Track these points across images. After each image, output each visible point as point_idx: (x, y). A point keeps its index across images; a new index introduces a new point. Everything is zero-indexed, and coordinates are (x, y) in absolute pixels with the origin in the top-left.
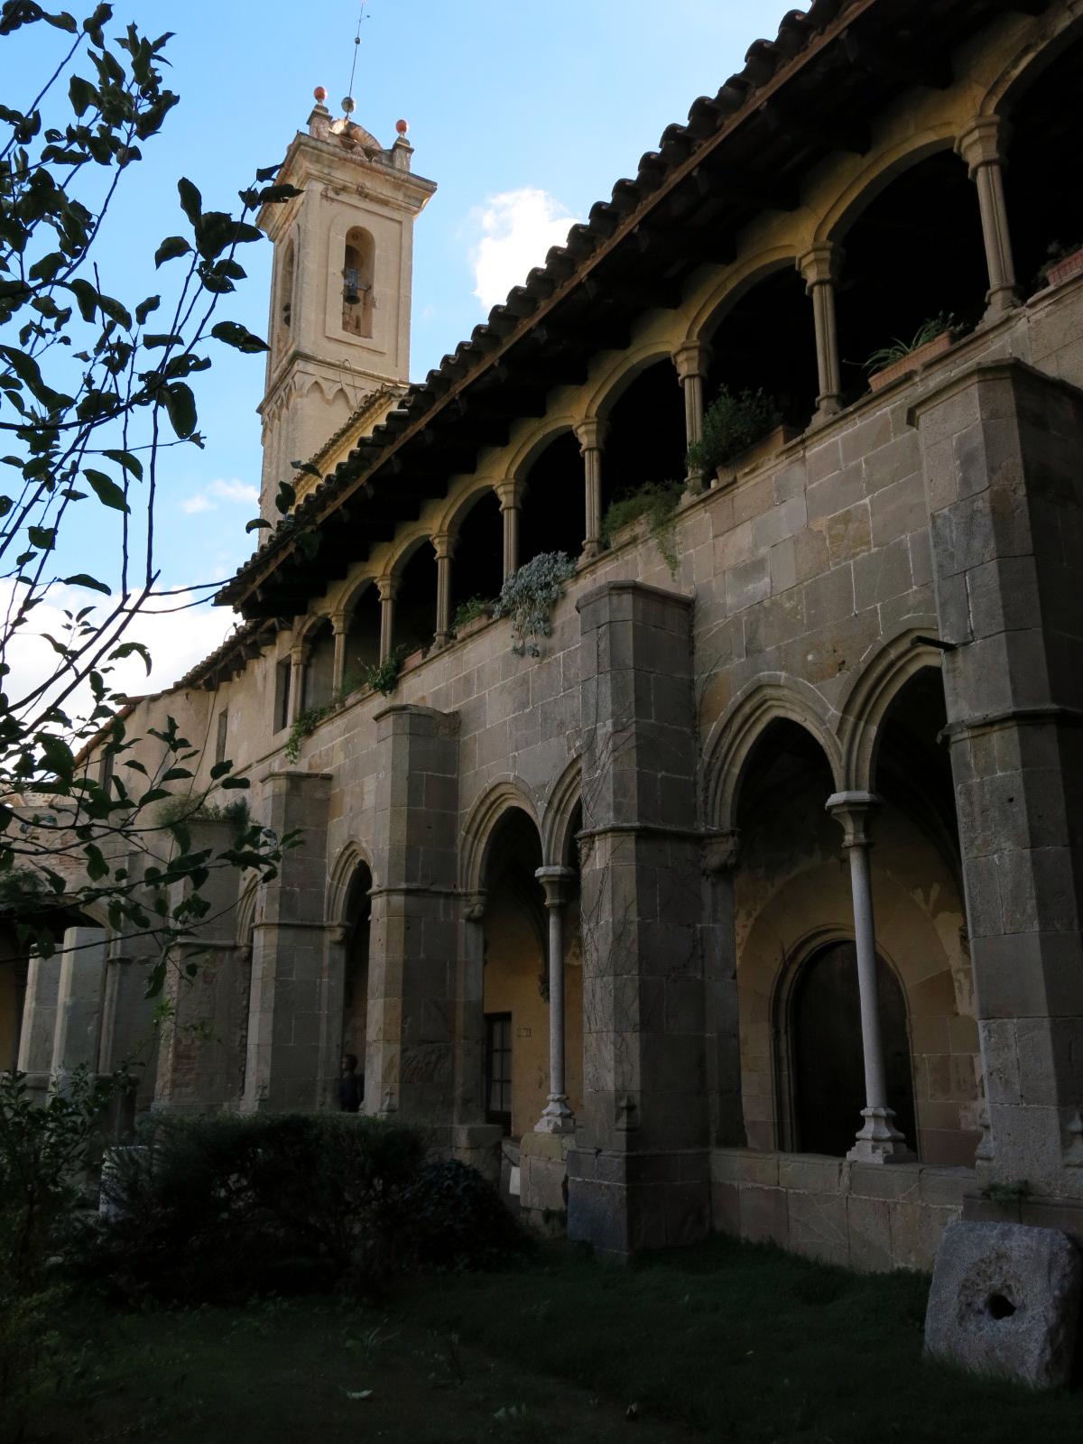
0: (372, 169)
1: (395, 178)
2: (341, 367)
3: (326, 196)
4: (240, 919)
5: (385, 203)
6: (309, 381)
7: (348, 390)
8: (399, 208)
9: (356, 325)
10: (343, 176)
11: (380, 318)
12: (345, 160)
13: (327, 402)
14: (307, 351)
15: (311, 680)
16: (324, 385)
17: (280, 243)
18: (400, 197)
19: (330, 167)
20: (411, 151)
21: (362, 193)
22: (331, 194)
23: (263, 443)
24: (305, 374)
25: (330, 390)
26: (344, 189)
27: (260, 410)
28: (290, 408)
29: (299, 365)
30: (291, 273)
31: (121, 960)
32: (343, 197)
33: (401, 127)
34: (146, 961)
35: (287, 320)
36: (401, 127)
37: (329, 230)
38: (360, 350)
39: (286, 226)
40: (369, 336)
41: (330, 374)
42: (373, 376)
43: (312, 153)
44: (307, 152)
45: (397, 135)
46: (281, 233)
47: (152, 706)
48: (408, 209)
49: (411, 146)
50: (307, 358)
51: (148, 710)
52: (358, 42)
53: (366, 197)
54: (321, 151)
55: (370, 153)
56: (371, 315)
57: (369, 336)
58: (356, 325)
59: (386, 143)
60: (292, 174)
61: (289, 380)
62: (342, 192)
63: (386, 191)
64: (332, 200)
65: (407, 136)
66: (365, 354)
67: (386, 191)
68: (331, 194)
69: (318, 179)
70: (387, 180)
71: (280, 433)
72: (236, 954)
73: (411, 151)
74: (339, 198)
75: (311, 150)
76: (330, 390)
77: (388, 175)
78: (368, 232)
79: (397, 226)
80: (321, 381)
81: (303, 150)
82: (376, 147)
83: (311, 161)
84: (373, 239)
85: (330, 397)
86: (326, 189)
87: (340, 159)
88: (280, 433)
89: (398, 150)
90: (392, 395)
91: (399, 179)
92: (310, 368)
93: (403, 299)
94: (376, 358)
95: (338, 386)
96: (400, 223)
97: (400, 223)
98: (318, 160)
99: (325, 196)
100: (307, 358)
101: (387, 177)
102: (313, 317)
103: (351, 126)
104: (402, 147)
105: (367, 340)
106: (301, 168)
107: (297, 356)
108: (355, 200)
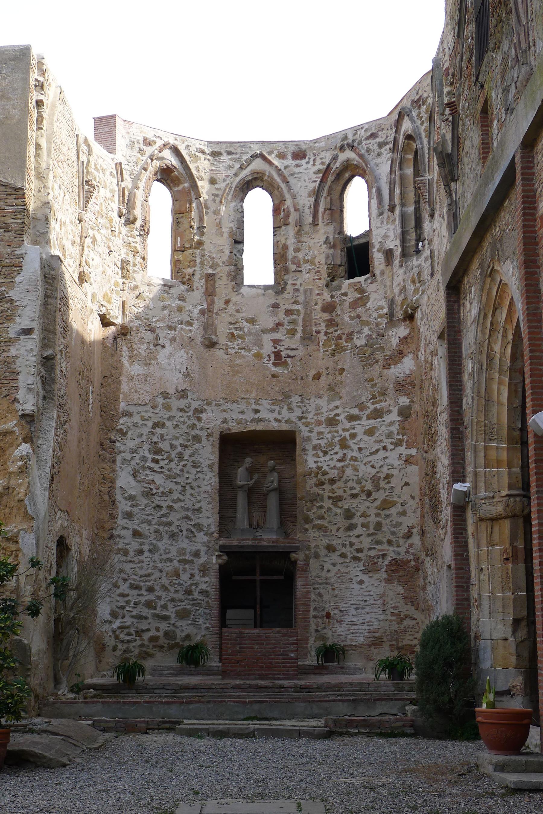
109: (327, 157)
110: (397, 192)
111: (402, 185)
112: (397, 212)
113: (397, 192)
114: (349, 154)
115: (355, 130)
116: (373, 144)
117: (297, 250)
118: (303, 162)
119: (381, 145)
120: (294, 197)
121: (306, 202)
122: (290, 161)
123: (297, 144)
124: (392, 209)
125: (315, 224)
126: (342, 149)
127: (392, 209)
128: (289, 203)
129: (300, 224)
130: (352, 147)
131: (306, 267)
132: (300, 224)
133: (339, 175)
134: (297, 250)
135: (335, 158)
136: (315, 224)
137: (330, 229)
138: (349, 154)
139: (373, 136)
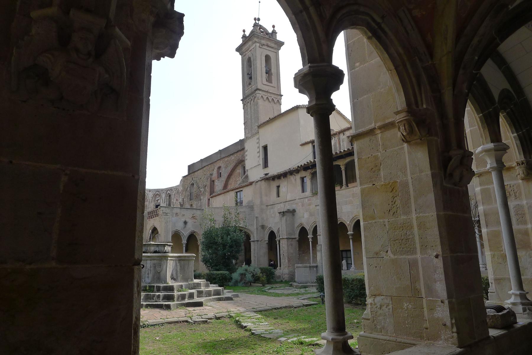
0: (270, 40)
1: (275, 41)
2: (267, 92)
3: (260, 47)
4: (296, 232)
5: (272, 48)
6: (261, 96)
7: (269, 97)
8: (275, 49)
9: (269, 80)
10: (263, 42)
11: (274, 78)
12: (264, 38)
13: (264, 101)
14: (259, 87)
15: (313, 183)
16: (264, 96)
17: (244, 56)
18: (276, 46)
19: (260, 39)
20: (277, 33)
21: (268, 46)
22: (261, 46)
23: (243, 109)
24: (259, 94)
25: (265, 98)
26: (264, 45)
27: (241, 100)
28: (255, 102)
29: (257, 92)
30: (251, 67)
31: (258, 241)
32: (264, 47)
33: (274, 27)
34: (261, 241)
35: (251, 78)
36: (274, 27)
37: (261, 56)
38: (270, 87)
39: (247, 52)
40: (272, 83)
41: (264, 93)
42: (274, 94)
43: (257, 36)
44: (256, 36)
45: (272, 29)
46: (244, 54)
47: (256, 183)
48: (278, 49)
49: (277, 32)
50: (259, 90)
51: (256, 184)
52: (260, 2)
53: (268, 46)
54: (259, 36)
55: (267, 33)
56: (272, 77)
57: (272, 83)
58: (269, 80)
59: (270, 30)
60: (250, 41)
61: (254, 94)
62: (263, 46)
63: (273, 45)
64: (261, 48)
65: (275, 29)
66: (271, 88)
67: (273, 45)
68: (261, 46)
69: (258, 42)
70: (273, 42)
71: (251, 108)
72: (296, 239)
73: (277, 33)
74: (262, 47)
75: (256, 36)
76: (265, 98)
77: (273, 41)
78: (269, 55)
79: (275, 53)
80: (263, 95)
81: (255, 36)
82: (267, 32)
83: (256, 39)
84: (271, 58)
85: (265, 100)
86: (260, 45)
87: (263, 37)
88: (251, 108)
89: (274, 33)
90: (299, 107)
91: (276, 42)
92: (260, 92)
93: (278, 73)
94: (274, 89)
95: (267, 96)
96: (276, 53)
97: (276, 53)
98: (258, 38)
99: (259, 47)
100: (259, 90)
101: (274, 41)
102: (260, 79)
103: (260, 26)
104: (274, 32)
105: (271, 84)
106: (253, 40)
107: (257, 89)
108: (266, 47)
109: (154, 192)
110: (166, 200)
111: (167, 200)
112: (166, 203)
113: (166, 200)
114: (158, 193)
115: (159, 189)
116: (162, 192)
117: (149, 205)
118: (150, 192)
119: (163, 192)
120: (149, 197)
121: (151, 199)
122: (148, 192)
123: (149, 189)
124: (165, 202)
125: (152, 202)
126: (157, 192)
127: (165, 202)
128: (148, 198)
129: (149, 202)
130: (158, 192)
131: (150, 208)
132: (149, 202)
133: (156, 195)
134: (149, 205)
135: (156, 193)
136: (152, 202)
137: (154, 203)
138: (158, 193)
139: (162, 191)
